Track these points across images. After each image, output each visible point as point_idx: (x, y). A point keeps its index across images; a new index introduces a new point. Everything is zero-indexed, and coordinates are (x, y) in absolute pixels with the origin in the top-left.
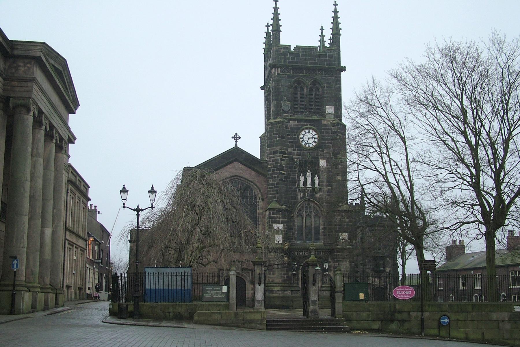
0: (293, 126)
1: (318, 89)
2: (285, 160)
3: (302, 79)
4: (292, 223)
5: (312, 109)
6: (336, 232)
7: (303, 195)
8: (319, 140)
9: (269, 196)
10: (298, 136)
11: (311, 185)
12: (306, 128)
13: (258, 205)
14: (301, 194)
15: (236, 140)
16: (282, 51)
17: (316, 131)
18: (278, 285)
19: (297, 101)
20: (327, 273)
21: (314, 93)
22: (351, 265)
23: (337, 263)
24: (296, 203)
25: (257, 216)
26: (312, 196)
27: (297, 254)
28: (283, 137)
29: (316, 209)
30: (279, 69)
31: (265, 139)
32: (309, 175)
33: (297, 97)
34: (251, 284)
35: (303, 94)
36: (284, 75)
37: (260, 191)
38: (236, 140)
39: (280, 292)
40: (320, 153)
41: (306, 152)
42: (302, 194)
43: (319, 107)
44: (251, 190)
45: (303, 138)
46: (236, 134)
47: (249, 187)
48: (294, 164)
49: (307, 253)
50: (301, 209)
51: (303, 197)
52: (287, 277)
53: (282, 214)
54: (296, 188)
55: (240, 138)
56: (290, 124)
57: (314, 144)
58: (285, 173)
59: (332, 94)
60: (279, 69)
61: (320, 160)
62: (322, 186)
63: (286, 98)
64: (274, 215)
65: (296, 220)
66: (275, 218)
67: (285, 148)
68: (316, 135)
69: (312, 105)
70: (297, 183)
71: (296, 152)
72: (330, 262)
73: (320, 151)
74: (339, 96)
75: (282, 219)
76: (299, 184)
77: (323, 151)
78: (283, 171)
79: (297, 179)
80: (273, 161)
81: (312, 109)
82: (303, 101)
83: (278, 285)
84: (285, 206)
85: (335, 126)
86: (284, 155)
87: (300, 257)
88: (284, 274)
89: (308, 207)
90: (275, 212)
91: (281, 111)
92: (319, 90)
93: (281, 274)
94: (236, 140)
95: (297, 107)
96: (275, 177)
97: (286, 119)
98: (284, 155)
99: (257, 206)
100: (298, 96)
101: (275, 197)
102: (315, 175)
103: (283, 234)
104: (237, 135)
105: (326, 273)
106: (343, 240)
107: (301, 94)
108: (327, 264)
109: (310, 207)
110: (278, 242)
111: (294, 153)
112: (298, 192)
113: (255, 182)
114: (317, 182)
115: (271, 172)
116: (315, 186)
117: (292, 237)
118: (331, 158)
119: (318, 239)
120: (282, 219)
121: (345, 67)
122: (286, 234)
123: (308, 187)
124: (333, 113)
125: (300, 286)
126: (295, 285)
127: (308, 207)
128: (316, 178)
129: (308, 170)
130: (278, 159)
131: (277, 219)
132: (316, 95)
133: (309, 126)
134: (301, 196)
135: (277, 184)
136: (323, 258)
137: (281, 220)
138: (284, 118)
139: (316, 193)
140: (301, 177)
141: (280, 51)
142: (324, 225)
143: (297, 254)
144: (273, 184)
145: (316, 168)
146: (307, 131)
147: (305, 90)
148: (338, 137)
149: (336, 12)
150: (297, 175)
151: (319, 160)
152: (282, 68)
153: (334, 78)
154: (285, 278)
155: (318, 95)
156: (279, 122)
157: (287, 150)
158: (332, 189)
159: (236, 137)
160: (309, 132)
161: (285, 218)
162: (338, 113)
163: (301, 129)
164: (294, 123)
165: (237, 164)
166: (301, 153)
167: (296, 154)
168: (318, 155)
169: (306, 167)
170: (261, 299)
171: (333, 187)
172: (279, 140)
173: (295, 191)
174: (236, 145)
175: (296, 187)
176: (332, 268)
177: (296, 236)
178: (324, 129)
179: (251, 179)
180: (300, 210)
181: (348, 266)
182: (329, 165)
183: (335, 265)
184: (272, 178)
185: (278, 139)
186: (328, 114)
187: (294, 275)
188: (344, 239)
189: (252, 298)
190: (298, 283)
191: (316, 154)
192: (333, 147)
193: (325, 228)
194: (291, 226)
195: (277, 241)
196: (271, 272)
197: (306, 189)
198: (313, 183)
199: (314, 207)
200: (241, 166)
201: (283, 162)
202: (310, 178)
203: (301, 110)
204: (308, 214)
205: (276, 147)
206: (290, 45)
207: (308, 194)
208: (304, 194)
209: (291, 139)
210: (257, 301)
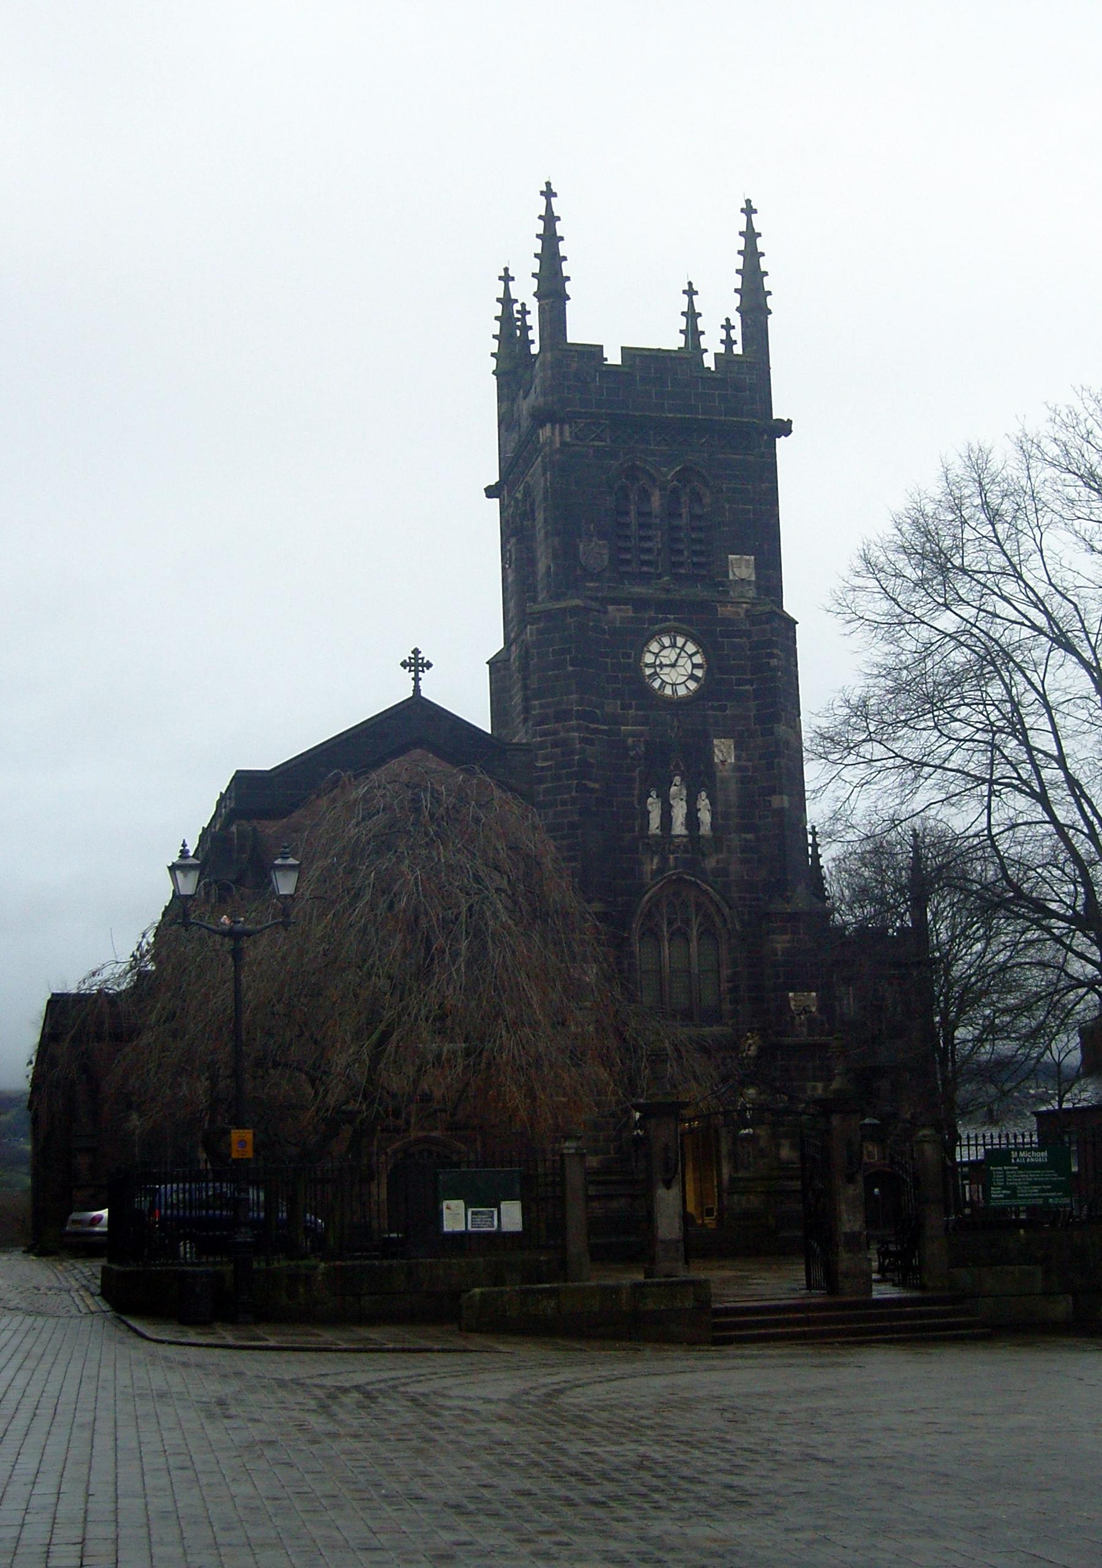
0: (618, 625)
1: (697, 498)
5: (681, 564)
8: (707, 673)
11: (687, 829)
14: (652, 861)
15: (417, 672)
16: (575, 365)
17: (697, 642)
19: (627, 538)
20: (751, 1130)
21: (684, 511)
30: (567, 427)
31: (507, 668)
32: (677, 789)
33: (628, 525)
35: (650, 514)
38: (417, 672)
43: (703, 560)
46: (416, 652)
51: (660, 871)
55: (429, 665)
57: (693, 685)
58: (597, 786)
60: (567, 427)
61: (716, 742)
63: (592, 526)
68: (698, 656)
70: (637, 823)
73: (712, 708)
77: (723, 708)
80: (555, 745)
81: (681, 564)
82: (649, 539)
86: (592, 726)
92: (700, 500)
94: (417, 675)
95: (628, 557)
97: (596, 599)
98: (592, 726)
100: (633, 518)
102: (700, 793)
104: (420, 656)
105: (747, 1131)
107: (640, 514)
114: (705, 816)
121: (790, 422)
123: (679, 836)
124: (753, 578)
128: (703, 802)
134: (654, 867)
138: (590, 598)
140: (650, 800)
146: (666, 641)
148: (774, 662)
149: (750, 235)
150: (636, 792)
155: (699, 517)
156: (574, 611)
159: (416, 664)
160: (673, 645)
167: (631, 721)
170: (674, 1236)
174: (417, 689)
175: (636, 834)
180: (649, 915)
187: (637, 1140)
197: (671, 843)
199: (698, 906)
202: (684, 804)
203: (645, 569)
204: (679, 929)
206: (602, 346)
208: (664, 860)
210: (662, 1242)
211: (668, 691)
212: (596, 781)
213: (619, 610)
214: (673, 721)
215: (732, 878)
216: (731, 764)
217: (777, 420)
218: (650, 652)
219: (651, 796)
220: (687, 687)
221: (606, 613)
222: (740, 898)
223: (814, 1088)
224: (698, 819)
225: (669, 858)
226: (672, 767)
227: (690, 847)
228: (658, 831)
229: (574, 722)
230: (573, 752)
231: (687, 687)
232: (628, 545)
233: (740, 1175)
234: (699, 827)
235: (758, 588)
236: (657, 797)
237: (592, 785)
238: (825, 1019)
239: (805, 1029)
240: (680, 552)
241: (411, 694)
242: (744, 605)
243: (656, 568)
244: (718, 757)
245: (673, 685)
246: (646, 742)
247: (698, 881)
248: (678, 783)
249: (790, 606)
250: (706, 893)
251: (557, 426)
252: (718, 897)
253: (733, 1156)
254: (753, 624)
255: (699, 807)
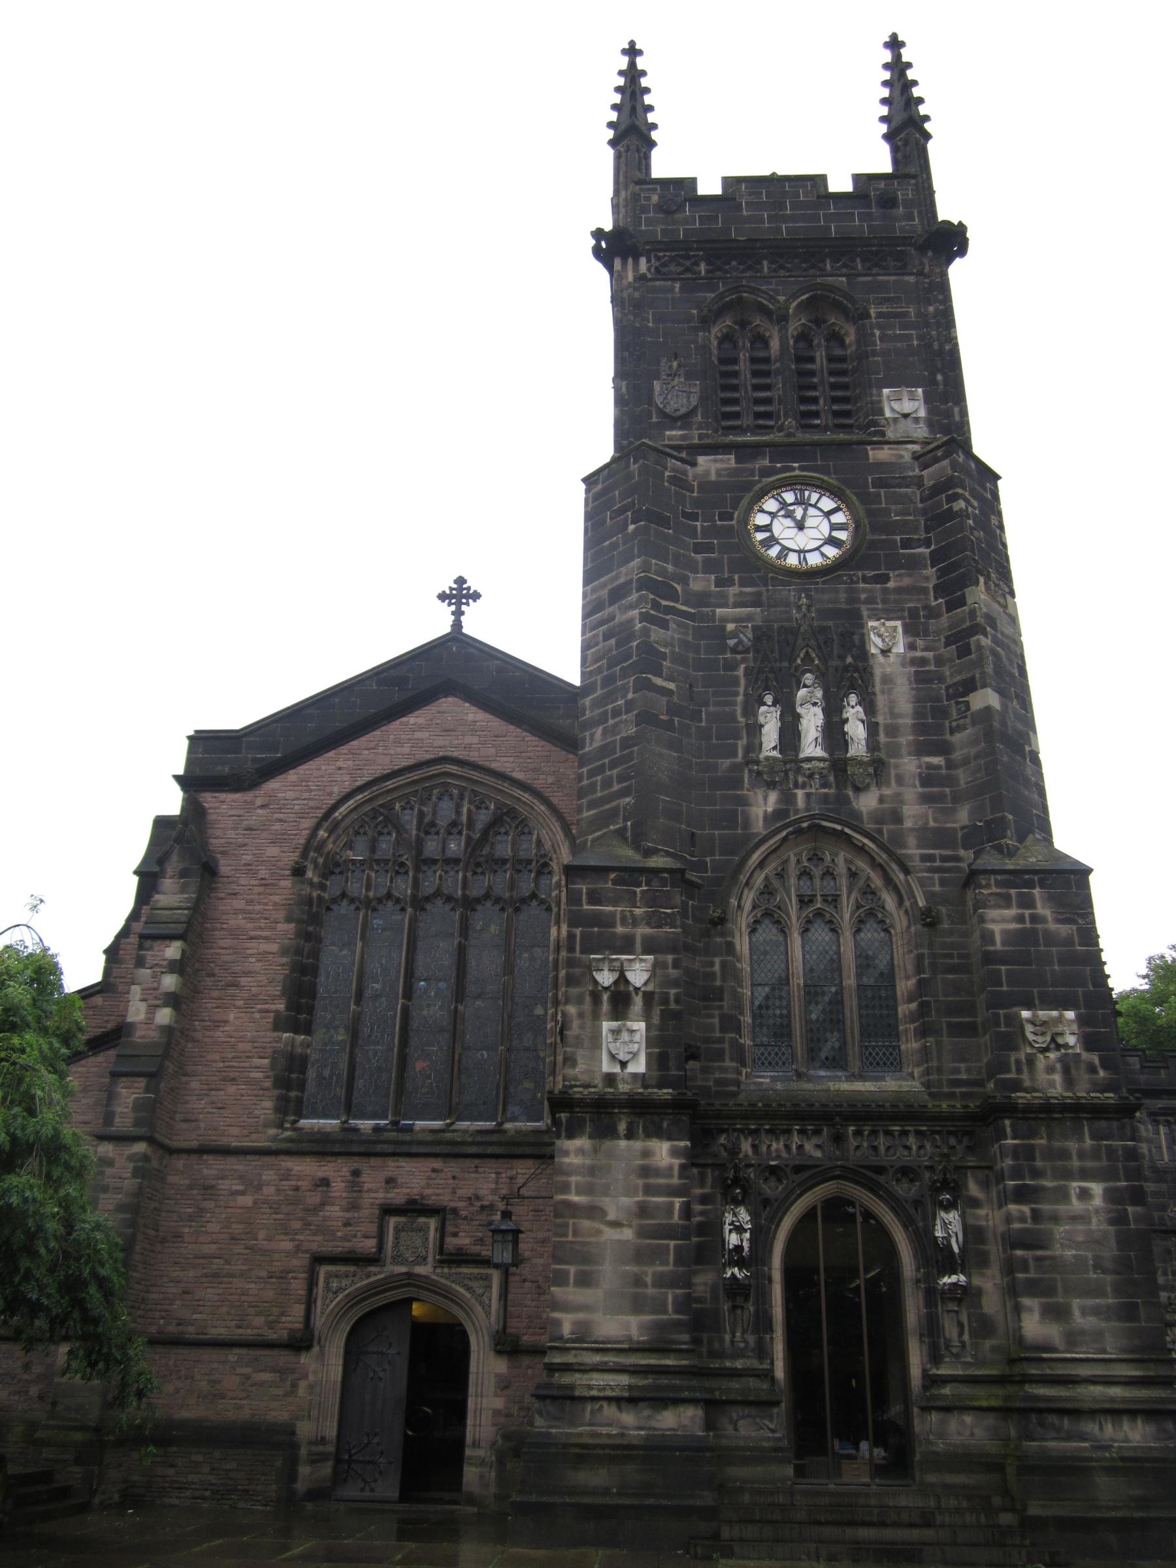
0: (713, 477)
1: (836, 338)
2: (672, 625)
3: (753, 291)
4: (717, 960)
5: (816, 414)
6: (997, 1001)
7: (779, 801)
9: (585, 814)
10: (745, 520)
12: (789, 484)
13: (553, 905)
14: (765, 798)
15: (459, 604)
16: (655, 198)
17: (834, 493)
18: (611, 1359)
19: (735, 388)
20: (962, 1278)
22: (1119, 1220)
23: (1026, 1209)
24: (742, 845)
25: (551, 958)
26: (840, 807)
27: (754, 1146)
28: (663, 521)
29: (861, 883)
33: (735, 374)
34: (499, 1352)
35: (767, 360)
36: (669, 283)
37: (566, 827)
39: (628, 1418)
40: (864, 590)
41: (789, 592)
42: (773, 797)
44: (523, 827)
45: (767, 528)
47: (511, 812)
48: (723, 648)
49: (815, 1140)
50: (776, 883)
51: (779, 814)
52: (683, 1305)
53: (652, 900)
54: (735, 768)
56: (699, 469)
57: (832, 552)
58: (672, 686)
59: (910, 337)
62: (894, 751)
64: (599, 903)
65: (742, 944)
66: (606, 921)
67: (670, 568)
69: (815, 400)
70: (741, 744)
71: (733, 590)
72: (975, 1203)
73: (865, 580)
74: (947, 347)
75: (648, 931)
76: (754, 745)
77: (885, 579)
78: (659, 674)
79: (740, 719)
81: (816, 414)
82: (767, 387)
83: (611, 1359)
84: (668, 854)
85: (937, 460)
86: (664, 603)
87: (774, 1171)
88: (661, 1282)
89: (817, 872)
90: (610, 885)
91: (654, 420)
93: (638, 1281)
96: (616, 713)
99: (549, 909)
100: (743, 366)
101: (613, 815)
103: (656, 1020)
105: (954, 1279)
106: (1052, 1056)
107: (754, 360)
108: (953, 1217)
109: (829, 873)
110: (624, 1064)
111: (723, 596)
112: (753, 787)
113: (538, 784)
115: (599, 692)
116: (852, 752)
117: (721, 1040)
118: (933, 613)
119: (892, 1062)
120: (648, 931)
122: (676, 1016)
123: (809, 759)
124: (922, 413)
125: (780, 1373)
126: (739, 1364)
127: (817, 872)
129: (805, 672)
130: (631, 620)
131: (620, 929)
132: (831, 359)
133: (797, 473)
134: (770, 810)
135: (627, 743)
136: (927, 1175)
137: (642, 931)
139: (858, 790)
140: (763, 709)
141: (649, 199)
142: (919, 969)
143: (750, 1152)
144: (605, 750)
145: (849, 660)
146: (789, 497)
147: (775, 344)
150: (740, 699)
151: (862, 626)
152: (658, 259)
153: (912, 279)
154: (665, 1312)
155: (843, 359)
157: (684, 581)
158: (950, 765)
161: (669, 921)
162: (949, 414)
163: (757, 488)
164: (719, 466)
165: (450, 708)
166: (758, 595)
167: (731, 600)
168: (857, 601)
169: (792, 660)
171: (957, 755)
172: (635, 529)
173: (737, 783)
174: (457, 625)
176: (994, 1250)
177: (747, 1041)
178: (880, 483)
179: (519, 775)
180: (768, 891)
181: (1104, 1227)
182: (920, 643)
183: (1009, 1219)
184: (603, 719)
185: (631, 527)
186: (895, 420)
187: (735, 1290)
188: (1058, 1047)
189: (494, 1444)
190: (763, 1351)
191: (843, 596)
192: (935, 559)
193: (922, 986)
194: (713, 975)
195: (613, 1057)
196: (572, 1269)
197: (799, 770)
198: (834, 732)
199: (853, 875)
200: (471, 717)
201: (656, 633)
202: (818, 711)
203: (761, 422)
204: (819, 914)
205: (623, 570)
207: (808, 795)
208: (787, 798)
209: (706, 532)
211: (792, 560)
212: (669, 679)
213: (716, 461)
214: (800, 598)
215: (908, 824)
216: (898, 655)
217: (944, 222)
218: (763, 511)
219: (764, 704)
220: (823, 555)
221: (694, 464)
222: (925, 858)
223: (1085, 1194)
224: (845, 734)
225: (795, 795)
226: (799, 661)
227: (832, 778)
228: (775, 754)
229: (634, 597)
230: (631, 636)
231: (823, 555)
232: (736, 395)
233: (942, 1372)
234: (846, 743)
235: (930, 424)
236: (774, 704)
237: (658, 681)
238: (1097, 1062)
239: (1057, 1078)
240: (815, 400)
241: (448, 630)
242: (910, 446)
243: (779, 418)
244: (875, 644)
245: (799, 552)
246: (754, 628)
247: (847, 830)
248: (808, 682)
249: (984, 446)
250: (861, 850)
251: (630, 261)
252: (884, 856)
253: (931, 1329)
254: (925, 467)
255: (845, 716)
